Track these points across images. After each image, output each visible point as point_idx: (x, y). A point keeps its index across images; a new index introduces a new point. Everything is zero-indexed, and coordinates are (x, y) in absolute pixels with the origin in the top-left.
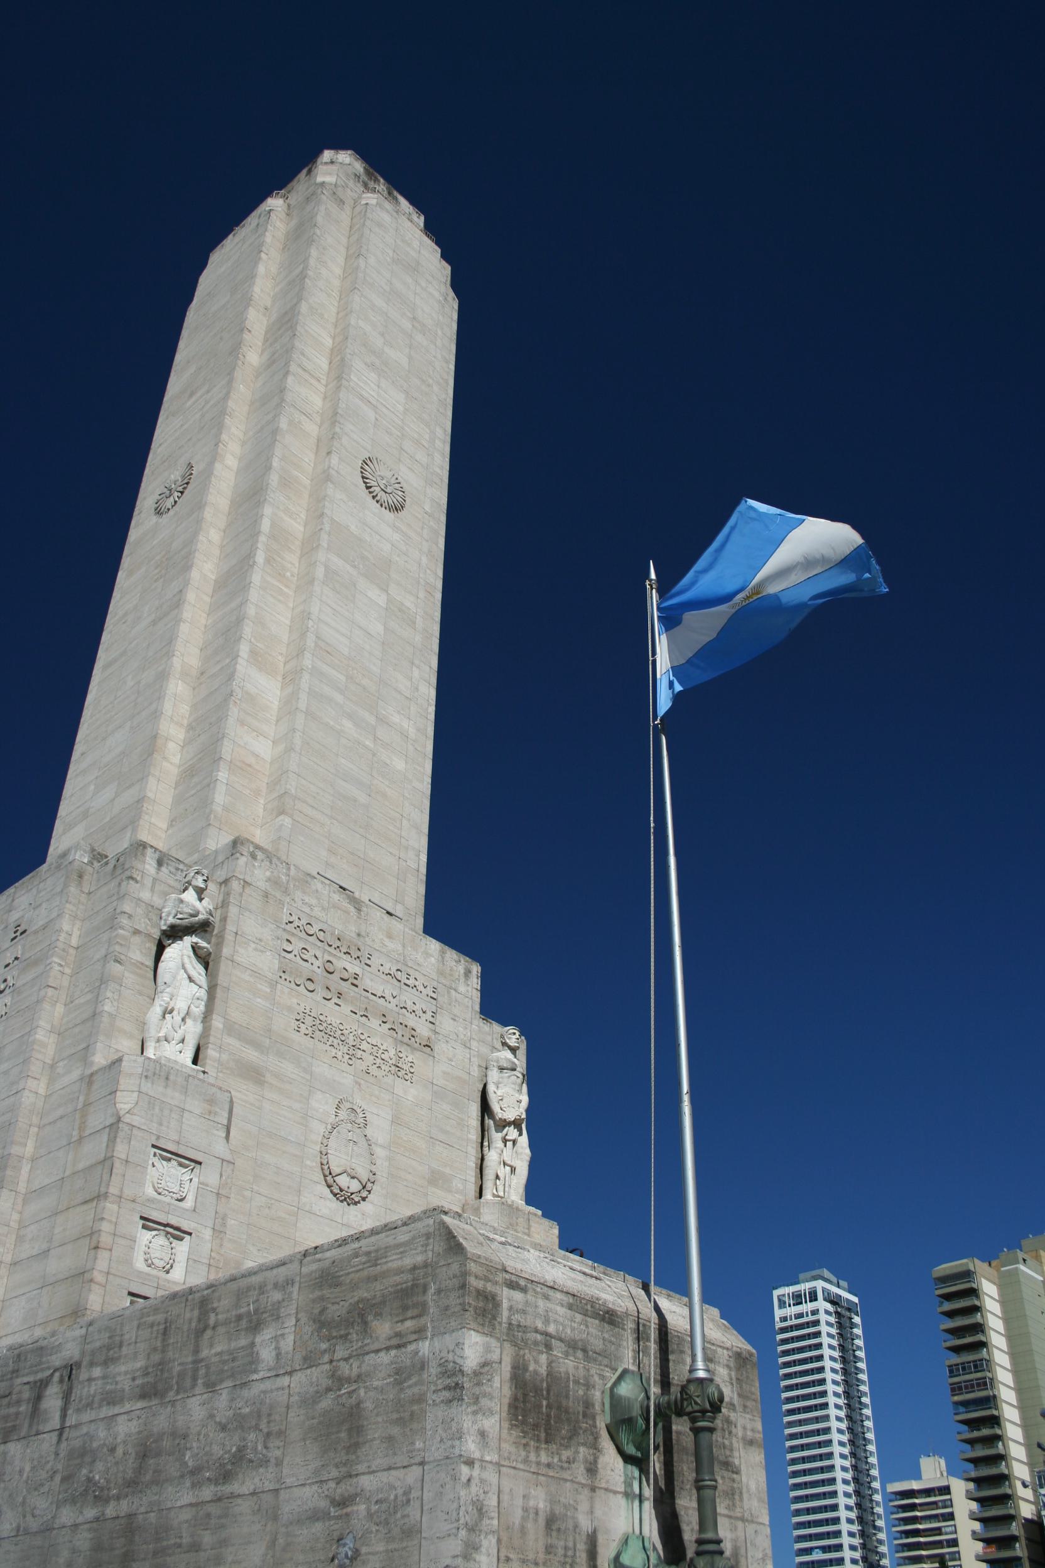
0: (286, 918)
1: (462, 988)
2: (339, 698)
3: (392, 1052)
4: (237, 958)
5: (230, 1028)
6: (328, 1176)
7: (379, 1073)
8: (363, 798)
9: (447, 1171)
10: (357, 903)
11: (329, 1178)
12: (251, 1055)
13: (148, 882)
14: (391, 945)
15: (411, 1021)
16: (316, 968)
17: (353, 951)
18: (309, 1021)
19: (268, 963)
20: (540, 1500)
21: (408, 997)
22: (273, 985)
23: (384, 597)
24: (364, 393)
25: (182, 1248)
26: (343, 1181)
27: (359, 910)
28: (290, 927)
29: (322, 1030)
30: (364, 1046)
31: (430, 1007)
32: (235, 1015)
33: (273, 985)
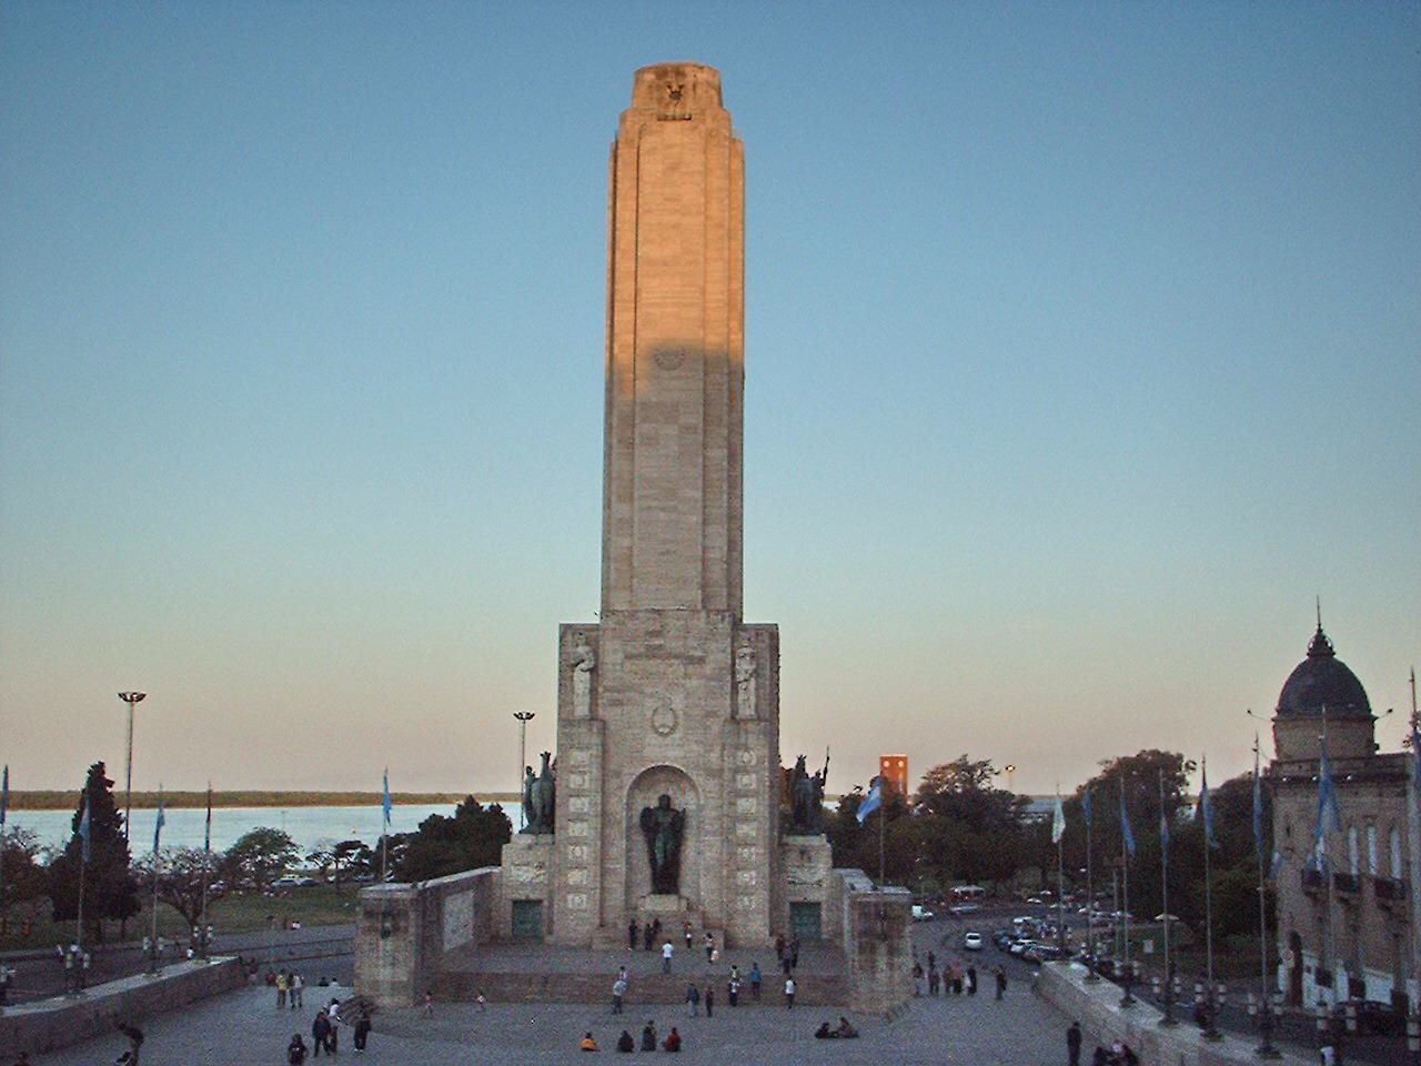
1: (721, 626)
2: (654, 504)
5: (607, 689)
8: (672, 547)
9: (716, 709)
13: (570, 644)
16: (642, 650)
17: (656, 634)
19: (620, 656)
20: (368, 924)
22: (622, 665)
24: (653, 301)
25: (586, 778)
26: (661, 730)
27: (660, 615)
33: (622, 665)
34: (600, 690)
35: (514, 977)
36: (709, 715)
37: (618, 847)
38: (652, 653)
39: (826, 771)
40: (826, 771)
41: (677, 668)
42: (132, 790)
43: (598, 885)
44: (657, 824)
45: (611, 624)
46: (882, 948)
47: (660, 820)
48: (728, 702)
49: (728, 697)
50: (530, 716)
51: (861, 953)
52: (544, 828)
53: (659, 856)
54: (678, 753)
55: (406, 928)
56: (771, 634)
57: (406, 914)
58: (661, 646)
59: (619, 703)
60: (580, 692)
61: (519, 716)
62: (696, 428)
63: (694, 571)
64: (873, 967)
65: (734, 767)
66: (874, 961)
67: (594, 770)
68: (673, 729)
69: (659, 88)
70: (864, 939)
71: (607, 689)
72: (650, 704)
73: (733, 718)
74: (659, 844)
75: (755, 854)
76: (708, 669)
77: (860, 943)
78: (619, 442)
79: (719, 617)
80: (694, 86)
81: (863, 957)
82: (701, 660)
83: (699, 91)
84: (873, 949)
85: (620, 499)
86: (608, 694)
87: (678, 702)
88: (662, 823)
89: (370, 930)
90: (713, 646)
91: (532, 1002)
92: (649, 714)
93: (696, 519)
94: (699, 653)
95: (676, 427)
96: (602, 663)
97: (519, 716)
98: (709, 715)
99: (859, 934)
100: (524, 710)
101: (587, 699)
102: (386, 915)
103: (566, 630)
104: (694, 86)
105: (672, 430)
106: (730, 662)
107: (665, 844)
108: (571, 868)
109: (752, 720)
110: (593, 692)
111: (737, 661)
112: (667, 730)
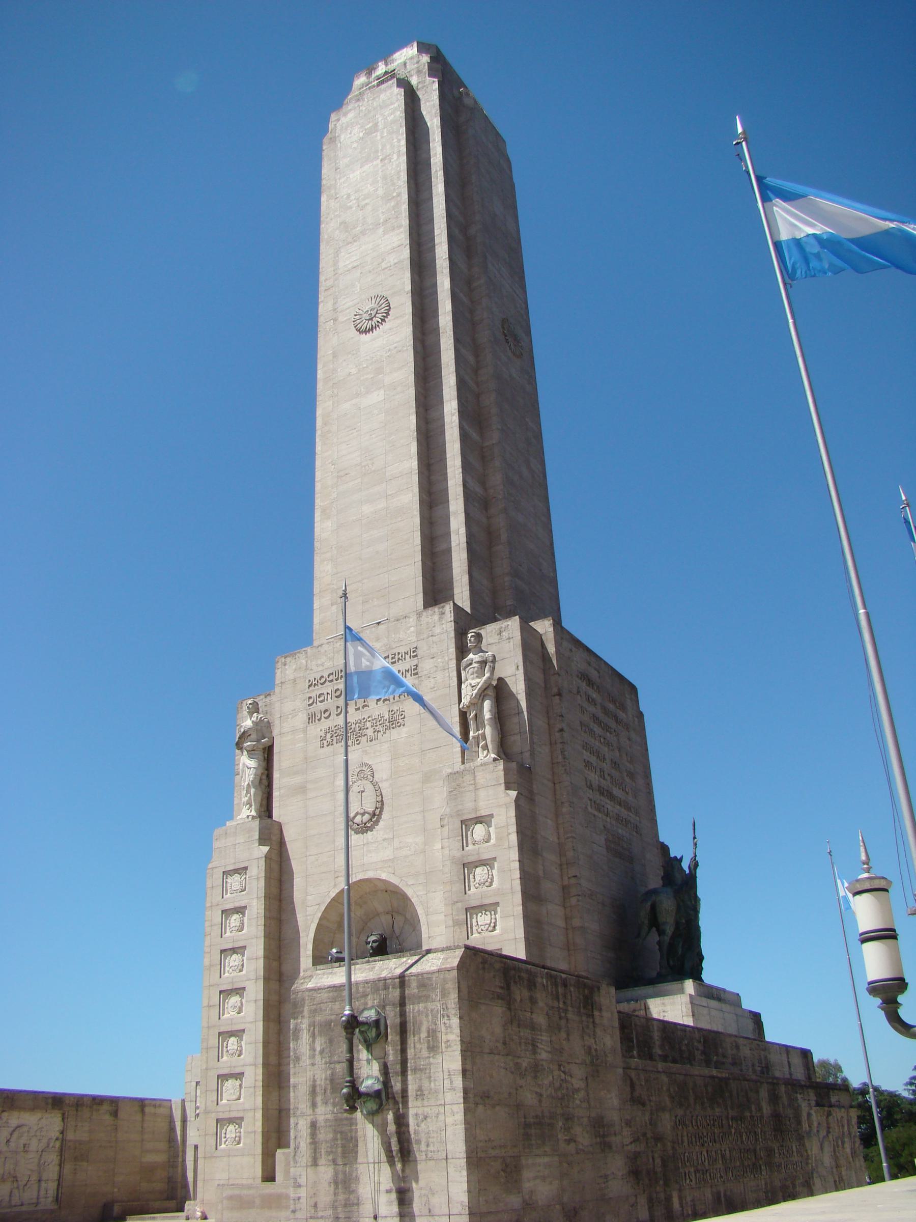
18: (329, 736)
33: (305, 731)
34: (276, 775)
36: (427, 778)
54: (388, 854)
59: (302, 789)
65: (458, 853)
67: (255, 902)
68: (376, 816)
79: (436, 617)
90: (426, 666)
95: (382, 392)
99: (313, 1092)
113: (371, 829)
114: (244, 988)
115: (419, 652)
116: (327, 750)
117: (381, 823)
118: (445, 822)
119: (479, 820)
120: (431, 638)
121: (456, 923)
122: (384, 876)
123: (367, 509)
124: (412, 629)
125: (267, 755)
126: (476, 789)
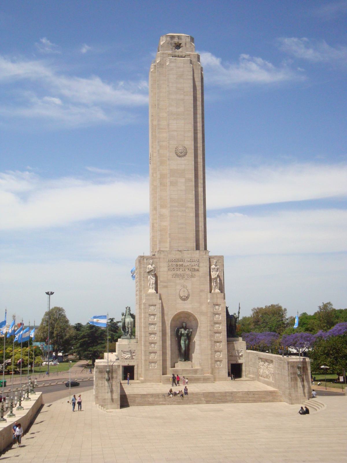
0: (168, 261)
1: (204, 257)
2: (177, 209)
3: (191, 274)
4: (160, 270)
5: (161, 282)
6: (181, 298)
7: (188, 278)
10: (180, 251)
11: (181, 298)
12: (165, 284)
13: (146, 264)
14: (189, 256)
15: (194, 267)
16: (175, 267)
18: (174, 275)
19: (166, 269)
20: (101, 376)
21: (193, 263)
23: (184, 179)
26: (183, 297)
28: (169, 262)
29: (177, 276)
30: (185, 275)
31: (197, 263)
32: (161, 279)
34: (159, 282)
35: (152, 395)
36: (202, 291)
37: (168, 342)
38: (179, 267)
39: (239, 313)
40: (239, 313)
41: (188, 272)
42: (35, 325)
43: (161, 358)
44: (181, 333)
45: (162, 256)
46: (299, 380)
47: (183, 332)
48: (209, 286)
49: (209, 284)
50: (52, 293)
51: (292, 381)
52: (133, 337)
53: (183, 346)
55: (116, 378)
56: (220, 259)
57: (116, 372)
58: (182, 264)
59: (166, 287)
60: (152, 283)
61: (47, 293)
62: (192, 180)
63: (193, 235)
64: (297, 386)
65: (212, 311)
66: (297, 384)
67: (159, 314)
68: (187, 298)
69: (171, 44)
70: (292, 376)
71: (161, 282)
72: (179, 287)
73: (210, 292)
74: (182, 342)
75: (223, 346)
76: (200, 273)
77: (291, 378)
78: (161, 184)
79: (204, 253)
80: (186, 44)
81: (293, 383)
82: (198, 270)
83: (187, 46)
84: (296, 380)
85: (162, 207)
86: (161, 283)
87: (189, 286)
88: (184, 334)
89: (102, 378)
90: (201, 265)
91: (163, 404)
92: (178, 291)
93: (193, 215)
94: (196, 267)
95: (184, 179)
96: (160, 271)
97: (47, 293)
98: (202, 291)
99: (291, 373)
100: (50, 291)
101: (154, 285)
102: (108, 372)
103: (142, 259)
104: (186, 44)
105: (183, 180)
106: (208, 270)
107: (185, 342)
108: (151, 353)
109: (218, 293)
110: (156, 283)
111: (212, 270)
112: (185, 297)
113: (186, 300)
114: (156, 333)
115: (200, 261)
116: (173, 278)
117: (189, 299)
118: (209, 304)
119: (217, 305)
120: (203, 258)
121: (211, 326)
122: (189, 311)
123: (180, 213)
124: (198, 254)
125: (156, 276)
126: (217, 298)
